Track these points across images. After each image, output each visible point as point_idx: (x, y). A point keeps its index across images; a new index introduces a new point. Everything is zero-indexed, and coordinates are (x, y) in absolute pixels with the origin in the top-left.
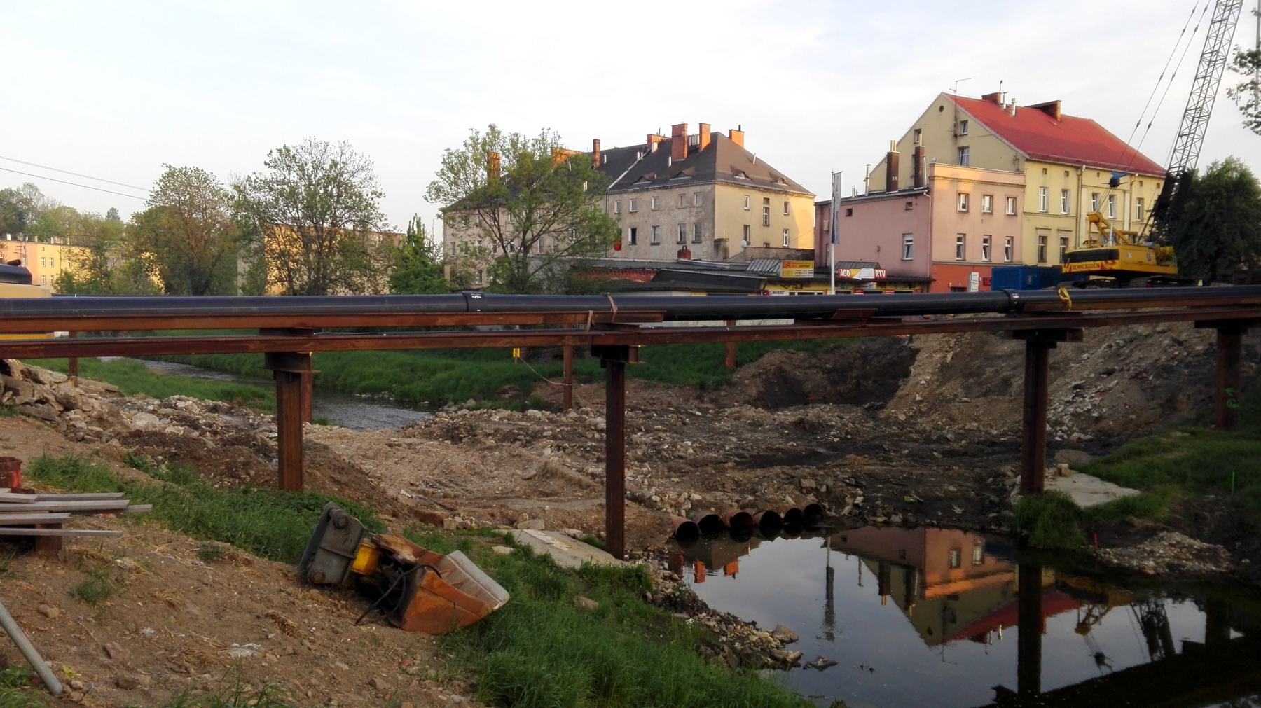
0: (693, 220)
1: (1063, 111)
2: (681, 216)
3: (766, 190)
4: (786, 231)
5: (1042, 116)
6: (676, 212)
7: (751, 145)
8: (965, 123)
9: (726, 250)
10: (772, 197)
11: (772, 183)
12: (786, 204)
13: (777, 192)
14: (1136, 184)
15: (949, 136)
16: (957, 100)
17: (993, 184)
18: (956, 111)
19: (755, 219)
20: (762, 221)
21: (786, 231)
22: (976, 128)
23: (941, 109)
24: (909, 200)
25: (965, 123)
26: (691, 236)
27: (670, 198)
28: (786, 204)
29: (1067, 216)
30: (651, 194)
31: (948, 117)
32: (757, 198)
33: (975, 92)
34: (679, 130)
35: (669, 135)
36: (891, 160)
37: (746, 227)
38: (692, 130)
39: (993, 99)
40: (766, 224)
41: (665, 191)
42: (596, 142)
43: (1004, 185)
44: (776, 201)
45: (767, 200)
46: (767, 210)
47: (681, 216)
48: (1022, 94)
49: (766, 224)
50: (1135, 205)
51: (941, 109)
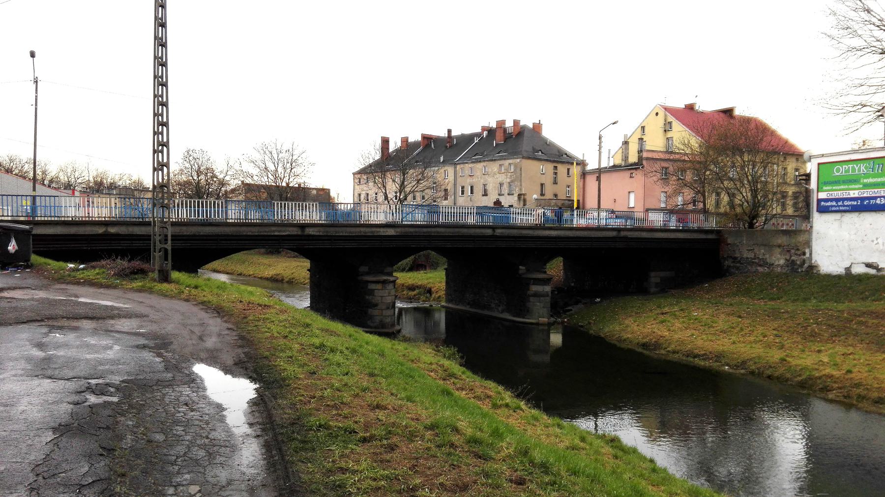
0: (508, 180)
2: (502, 178)
3: (554, 162)
5: (722, 115)
6: (498, 175)
7: (547, 133)
8: (670, 123)
9: (525, 201)
10: (559, 166)
11: (558, 157)
12: (568, 170)
15: (661, 131)
16: (666, 109)
18: (666, 115)
19: (548, 180)
20: (552, 180)
23: (657, 114)
25: (670, 123)
26: (505, 190)
27: (494, 167)
28: (568, 170)
30: (482, 164)
31: (660, 120)
32: (550, 167)
33: (681, 105)
34: (501, 123)
35: (494, 126)
37: (542, 185)
38: (509, 124)
39: (690, 108)
40: (555, 183)
42: (449, 131)
44: (562, 169)
45: (556, 168)
46: (556, 174)
47: (502, 178)
48: (708, 104)
49: (555, 183)
51: (657, 114)
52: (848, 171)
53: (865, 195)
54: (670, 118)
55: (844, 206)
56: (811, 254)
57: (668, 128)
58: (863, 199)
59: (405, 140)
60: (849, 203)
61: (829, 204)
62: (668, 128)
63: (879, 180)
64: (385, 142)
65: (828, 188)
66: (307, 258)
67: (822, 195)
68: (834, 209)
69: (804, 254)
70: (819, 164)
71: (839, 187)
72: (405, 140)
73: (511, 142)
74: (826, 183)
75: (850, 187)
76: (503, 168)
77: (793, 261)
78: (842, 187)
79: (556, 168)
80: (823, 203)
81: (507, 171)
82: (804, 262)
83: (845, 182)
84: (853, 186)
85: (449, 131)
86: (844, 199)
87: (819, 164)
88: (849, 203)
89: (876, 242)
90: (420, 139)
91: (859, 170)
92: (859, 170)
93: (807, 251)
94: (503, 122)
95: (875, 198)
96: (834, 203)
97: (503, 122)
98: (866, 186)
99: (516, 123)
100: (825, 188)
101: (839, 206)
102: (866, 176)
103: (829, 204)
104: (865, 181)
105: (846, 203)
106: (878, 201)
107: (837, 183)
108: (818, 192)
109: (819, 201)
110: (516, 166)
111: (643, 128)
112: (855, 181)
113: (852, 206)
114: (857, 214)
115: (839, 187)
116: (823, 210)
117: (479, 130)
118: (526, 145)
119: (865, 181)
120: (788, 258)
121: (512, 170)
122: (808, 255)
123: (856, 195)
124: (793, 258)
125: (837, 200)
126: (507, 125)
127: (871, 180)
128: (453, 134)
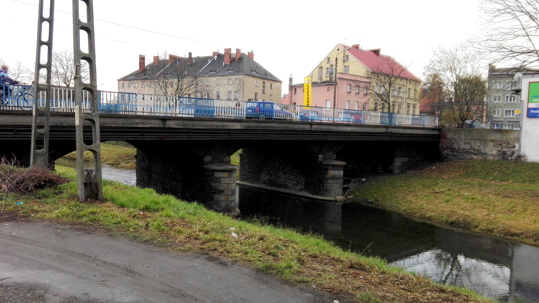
0: (235, 90)
1: (382, 53)
3: (264, 79)
4: (271, 96)
5: (373, 54)
7: (257, 59)
8: (347, 56)
10: (266, 82)
13: (268, 80)
14: (408, 83)
17: (360, 81)
19: (259, 91)
20: (262, 90)
21: (271, 96)
22: (352, 58)
23: (338, 50)
24: (329, 86)
27: (224, 80)
30: (216, 78)
32: (261, 82)
33: (350, 44)
34: (228, 51)
37: (256, 94)
38: (233, 52)
39: (356, 47)
40: (264, 93)
41: (222, 77)
42: (190, 54)
43: (363, 82)
45: (264, 83)
46: (264, 87)
47: (230, 88)
48: (366, 46)
49: (264, 93)
51: (338, 50)
54: (348, 53)
56: (520, 147)
57: (345, 59)
59: (156, 58)
62: (345, 59)
64: (142, 59)
67: (531, 105)
69: (514, 147)
70: (530, 83)
72: (156, 58)
73: (234, 63)
74: (535, 97)
76: (231, 81)
77: (504, 152)
79: (264, 83)
80: (532, 111)
81: (234, 83)
82: (513, 153)
85: (190, 54)
87: (530, 83)
90: (168, 58)
93: (517, 145)
94: (230, 50)
97: (230, 50)
99: (238, 51)
100: (534, 100)
108: (528, 103)
109: (529, 110)
110: (240, 81)
111: (329, 59)
117: (211, 54)
118: (246, 67)
120: (500, 149)
121: (237, 83)
122: (517, 148)
124: (504, 150)
126: (232, 53)
128: (193, 56)
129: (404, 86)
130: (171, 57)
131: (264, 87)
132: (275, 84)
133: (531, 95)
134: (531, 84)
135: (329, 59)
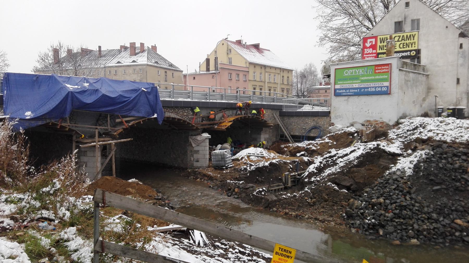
1: (261, 47)
10: (168, 71)
15: (225, 54)
23: (223, 44)
24: (213, 75)
29: (262, 81)
33: (234, 39)
36: (208, 61)
42: (100, 47)
45: (166, 72)
46: (166, 75)
50: (281, 78)
51: (223, 44)
52: (352, 73)
53: (362, 86)
55: (350, 92)
58: (360, 89)
59: (69, 51)
60: (353, 91)
61: (341, 91)
63: (370, 78)
64: (56, 52)
65: (341, 82)
66: (187, 143)
67: (337, 87)
68: (344, 94)
70: (336, 69)
71: (347, 82)
74: (340, 80)
75: (354, 82)
76: (135, 71)
78: (349, 82)
79: (166, 72)
80: (337, 91)
83: (350, 79)
84: (355, 82)
85: (100, 47)
86: (349, 89)
87: (336, 69)
88: (353, 91)
89: (367, 112)
90: (80, 51)
91: (359, 72)
92: (359, 72)
95: (368, 88)
96: (344, 91)
98: (363, 81)
99: (142, 45)
100: (339, 83)
101: (347, 93)
102: (363, 76)
103: (341, 91)
104: (362, 78)
105: (351, 91)
106: (369, 90)
107: (345, 79)
109: (335, 90)
111: (216, 52)
112: (357, 79)
113: (355, 92)
114: (357, 97)
115: (347, 82)
116: (337, 94)
119: (362, 78)
123: (357, 86)
125: (346, 89)
127: (365, 78)
128: (102, 49)
129: (278, 74)
130: (82, 49)
131: (166, 75)
132: (176, 74)
133: (336, 79)
134: (336, 70)
135: (216, 52)
